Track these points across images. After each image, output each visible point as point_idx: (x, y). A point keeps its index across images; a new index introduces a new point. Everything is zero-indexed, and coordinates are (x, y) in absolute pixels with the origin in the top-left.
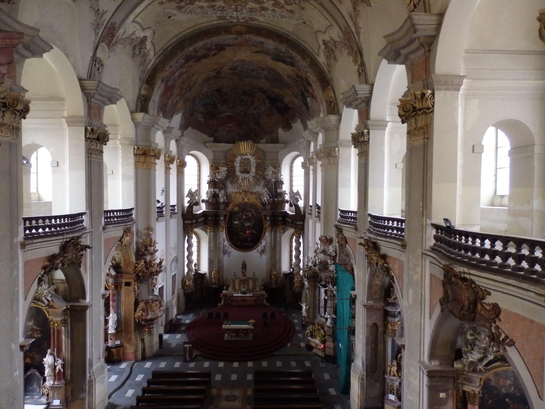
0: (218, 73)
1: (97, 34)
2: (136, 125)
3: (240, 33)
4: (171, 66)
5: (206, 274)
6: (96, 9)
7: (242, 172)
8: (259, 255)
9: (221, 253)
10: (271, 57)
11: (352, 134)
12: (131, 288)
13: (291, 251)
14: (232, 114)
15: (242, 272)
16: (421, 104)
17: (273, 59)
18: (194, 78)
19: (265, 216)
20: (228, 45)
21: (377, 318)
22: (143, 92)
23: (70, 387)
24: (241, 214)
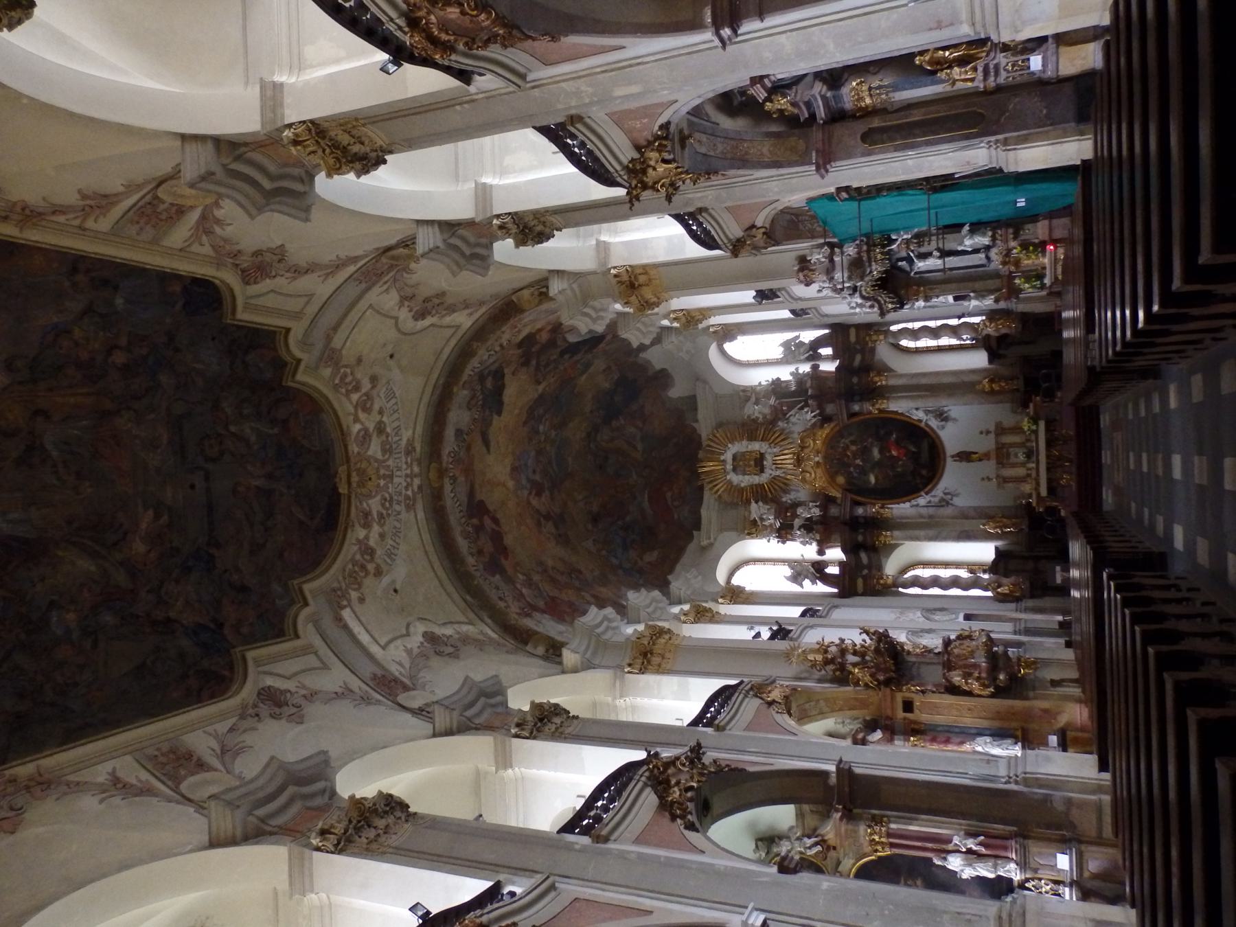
0: (548, 517)
1: (378, 702)
2: (587, 666)
3: (442, 473)
4: (500, 599)
5: (997, 548)
6: (334, 695)
7: (762, 471)
9: (948, 511)
10: (495, 417)
11: (517, 246)
12: (918, 701)
13: (940, 349)
14: (646, 492)
15: (980, 460)
16: (308, 142)
17: (499, 413)
18: (550, 563)
19: (852, 415)
20: (471, 494)
21: (849, 133)
22: (541, 650)
23: (1035, 830)
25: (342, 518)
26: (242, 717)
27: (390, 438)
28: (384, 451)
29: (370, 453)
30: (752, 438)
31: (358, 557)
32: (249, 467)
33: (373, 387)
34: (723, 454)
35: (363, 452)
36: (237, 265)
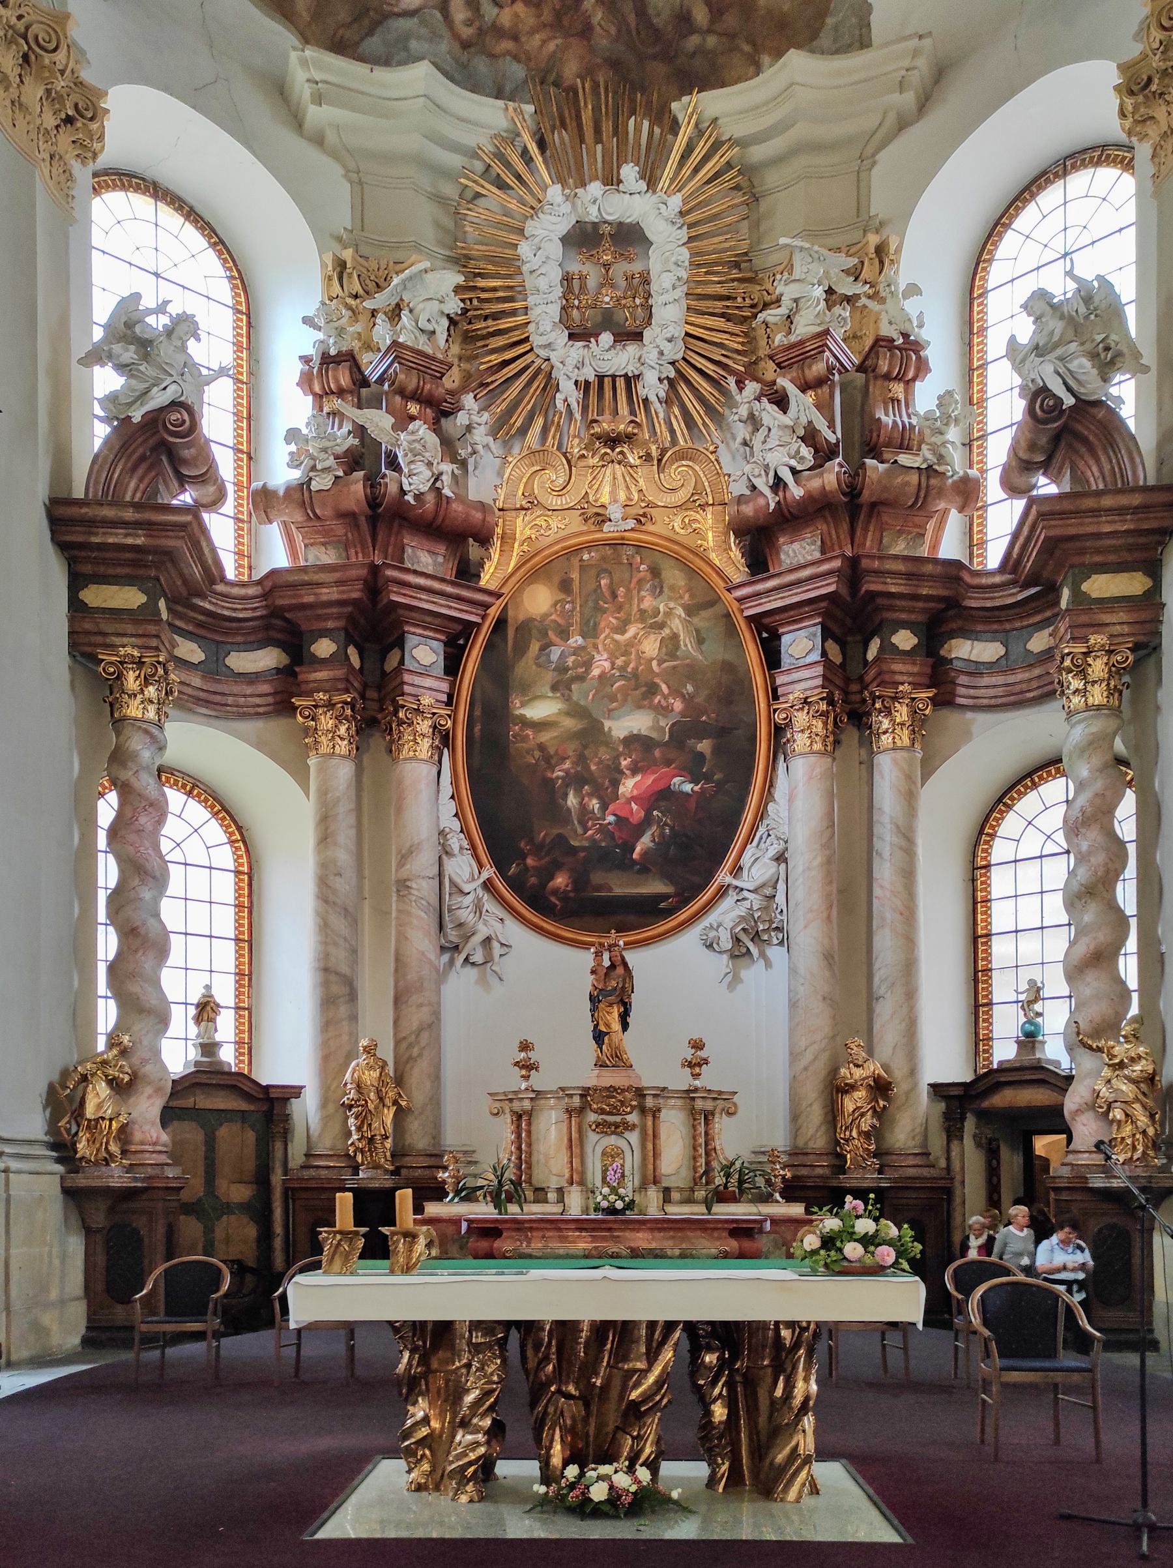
8: (722, 963)
24: (576, 640)
30: (697, 301)
34: (651, 183)
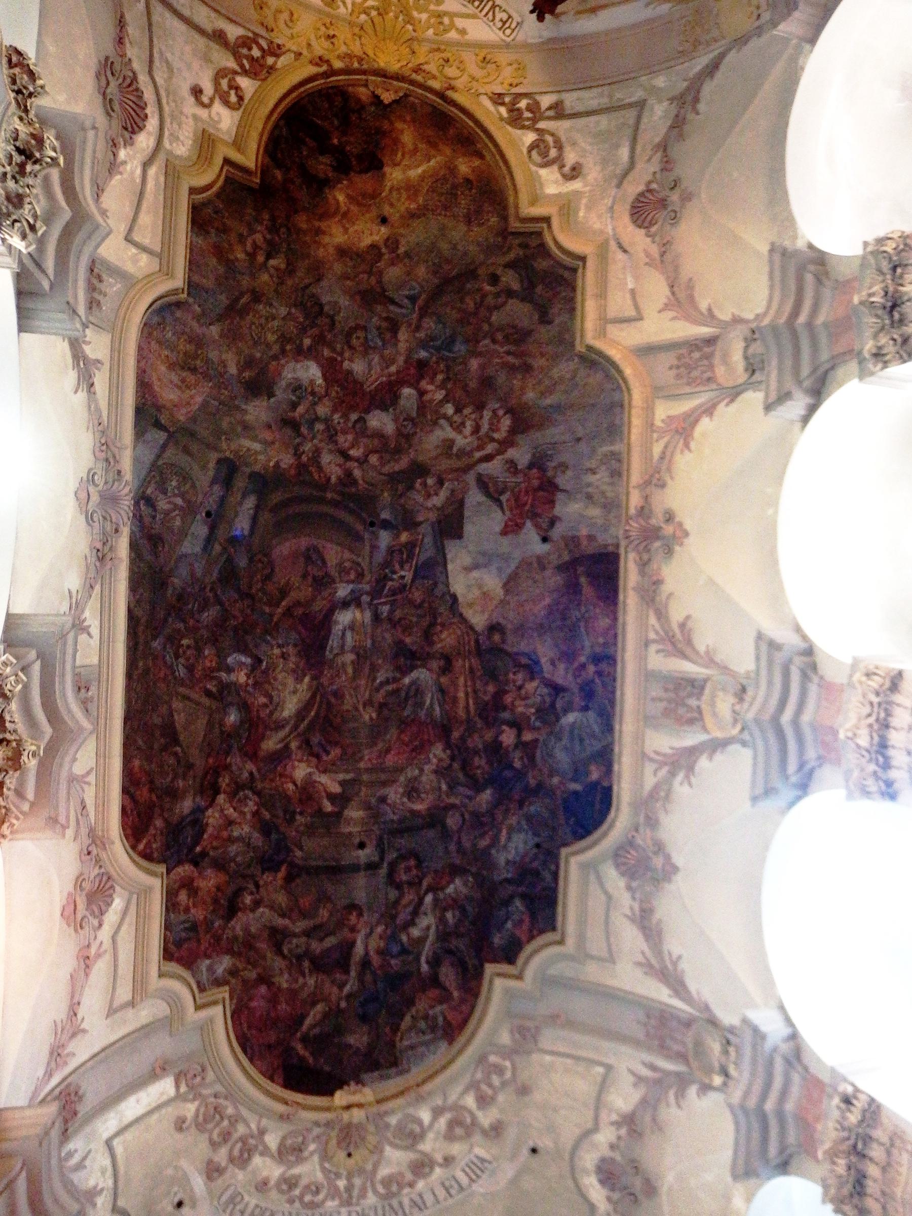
1: (49, 1074)
6: (75, 1001)
25: (299, 1097)
26: (92, 832)
27: (406, 1190)
28: (387, 1182)
29: (388, 1150)
31: (241, 1129)
32: (380, 929)
33: (485, 1133)
35: (389, 1135)
36: (637, 830)
